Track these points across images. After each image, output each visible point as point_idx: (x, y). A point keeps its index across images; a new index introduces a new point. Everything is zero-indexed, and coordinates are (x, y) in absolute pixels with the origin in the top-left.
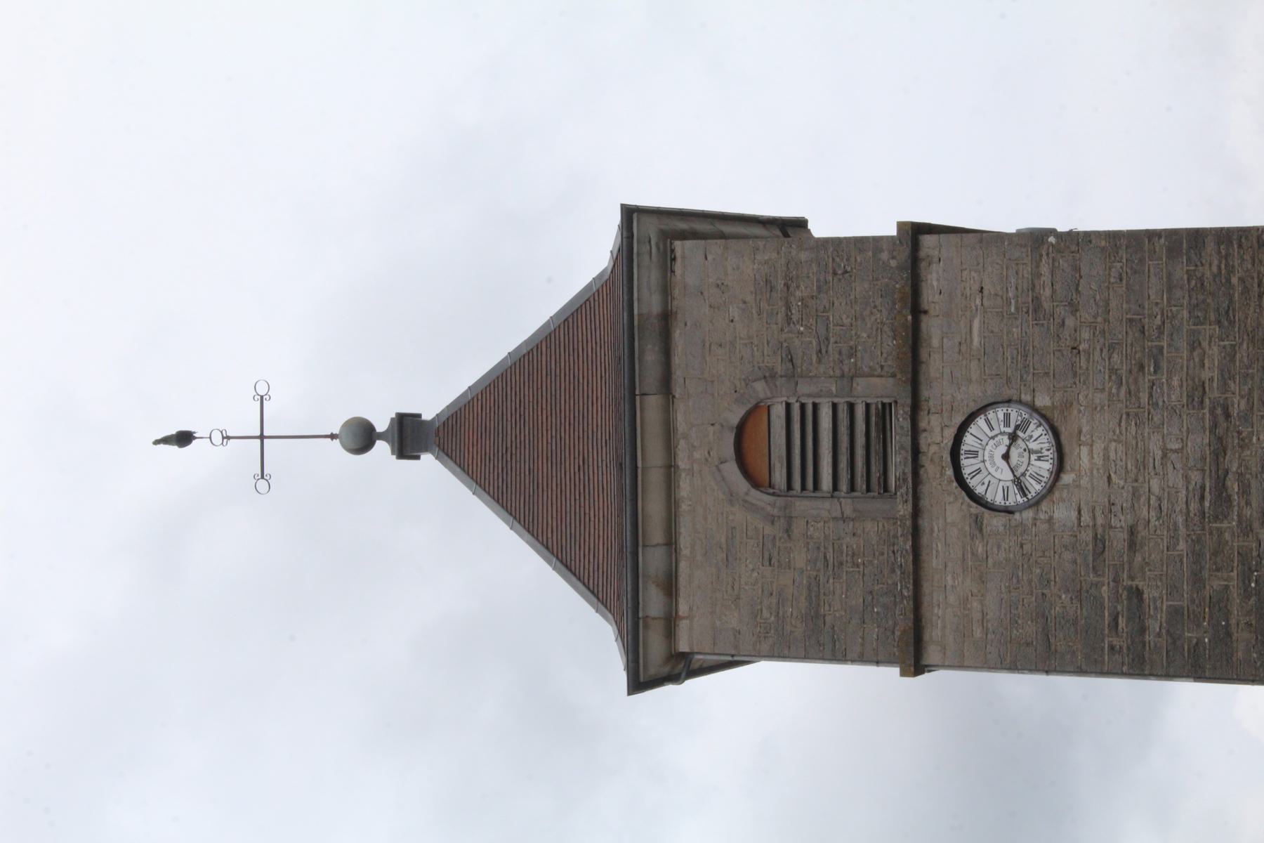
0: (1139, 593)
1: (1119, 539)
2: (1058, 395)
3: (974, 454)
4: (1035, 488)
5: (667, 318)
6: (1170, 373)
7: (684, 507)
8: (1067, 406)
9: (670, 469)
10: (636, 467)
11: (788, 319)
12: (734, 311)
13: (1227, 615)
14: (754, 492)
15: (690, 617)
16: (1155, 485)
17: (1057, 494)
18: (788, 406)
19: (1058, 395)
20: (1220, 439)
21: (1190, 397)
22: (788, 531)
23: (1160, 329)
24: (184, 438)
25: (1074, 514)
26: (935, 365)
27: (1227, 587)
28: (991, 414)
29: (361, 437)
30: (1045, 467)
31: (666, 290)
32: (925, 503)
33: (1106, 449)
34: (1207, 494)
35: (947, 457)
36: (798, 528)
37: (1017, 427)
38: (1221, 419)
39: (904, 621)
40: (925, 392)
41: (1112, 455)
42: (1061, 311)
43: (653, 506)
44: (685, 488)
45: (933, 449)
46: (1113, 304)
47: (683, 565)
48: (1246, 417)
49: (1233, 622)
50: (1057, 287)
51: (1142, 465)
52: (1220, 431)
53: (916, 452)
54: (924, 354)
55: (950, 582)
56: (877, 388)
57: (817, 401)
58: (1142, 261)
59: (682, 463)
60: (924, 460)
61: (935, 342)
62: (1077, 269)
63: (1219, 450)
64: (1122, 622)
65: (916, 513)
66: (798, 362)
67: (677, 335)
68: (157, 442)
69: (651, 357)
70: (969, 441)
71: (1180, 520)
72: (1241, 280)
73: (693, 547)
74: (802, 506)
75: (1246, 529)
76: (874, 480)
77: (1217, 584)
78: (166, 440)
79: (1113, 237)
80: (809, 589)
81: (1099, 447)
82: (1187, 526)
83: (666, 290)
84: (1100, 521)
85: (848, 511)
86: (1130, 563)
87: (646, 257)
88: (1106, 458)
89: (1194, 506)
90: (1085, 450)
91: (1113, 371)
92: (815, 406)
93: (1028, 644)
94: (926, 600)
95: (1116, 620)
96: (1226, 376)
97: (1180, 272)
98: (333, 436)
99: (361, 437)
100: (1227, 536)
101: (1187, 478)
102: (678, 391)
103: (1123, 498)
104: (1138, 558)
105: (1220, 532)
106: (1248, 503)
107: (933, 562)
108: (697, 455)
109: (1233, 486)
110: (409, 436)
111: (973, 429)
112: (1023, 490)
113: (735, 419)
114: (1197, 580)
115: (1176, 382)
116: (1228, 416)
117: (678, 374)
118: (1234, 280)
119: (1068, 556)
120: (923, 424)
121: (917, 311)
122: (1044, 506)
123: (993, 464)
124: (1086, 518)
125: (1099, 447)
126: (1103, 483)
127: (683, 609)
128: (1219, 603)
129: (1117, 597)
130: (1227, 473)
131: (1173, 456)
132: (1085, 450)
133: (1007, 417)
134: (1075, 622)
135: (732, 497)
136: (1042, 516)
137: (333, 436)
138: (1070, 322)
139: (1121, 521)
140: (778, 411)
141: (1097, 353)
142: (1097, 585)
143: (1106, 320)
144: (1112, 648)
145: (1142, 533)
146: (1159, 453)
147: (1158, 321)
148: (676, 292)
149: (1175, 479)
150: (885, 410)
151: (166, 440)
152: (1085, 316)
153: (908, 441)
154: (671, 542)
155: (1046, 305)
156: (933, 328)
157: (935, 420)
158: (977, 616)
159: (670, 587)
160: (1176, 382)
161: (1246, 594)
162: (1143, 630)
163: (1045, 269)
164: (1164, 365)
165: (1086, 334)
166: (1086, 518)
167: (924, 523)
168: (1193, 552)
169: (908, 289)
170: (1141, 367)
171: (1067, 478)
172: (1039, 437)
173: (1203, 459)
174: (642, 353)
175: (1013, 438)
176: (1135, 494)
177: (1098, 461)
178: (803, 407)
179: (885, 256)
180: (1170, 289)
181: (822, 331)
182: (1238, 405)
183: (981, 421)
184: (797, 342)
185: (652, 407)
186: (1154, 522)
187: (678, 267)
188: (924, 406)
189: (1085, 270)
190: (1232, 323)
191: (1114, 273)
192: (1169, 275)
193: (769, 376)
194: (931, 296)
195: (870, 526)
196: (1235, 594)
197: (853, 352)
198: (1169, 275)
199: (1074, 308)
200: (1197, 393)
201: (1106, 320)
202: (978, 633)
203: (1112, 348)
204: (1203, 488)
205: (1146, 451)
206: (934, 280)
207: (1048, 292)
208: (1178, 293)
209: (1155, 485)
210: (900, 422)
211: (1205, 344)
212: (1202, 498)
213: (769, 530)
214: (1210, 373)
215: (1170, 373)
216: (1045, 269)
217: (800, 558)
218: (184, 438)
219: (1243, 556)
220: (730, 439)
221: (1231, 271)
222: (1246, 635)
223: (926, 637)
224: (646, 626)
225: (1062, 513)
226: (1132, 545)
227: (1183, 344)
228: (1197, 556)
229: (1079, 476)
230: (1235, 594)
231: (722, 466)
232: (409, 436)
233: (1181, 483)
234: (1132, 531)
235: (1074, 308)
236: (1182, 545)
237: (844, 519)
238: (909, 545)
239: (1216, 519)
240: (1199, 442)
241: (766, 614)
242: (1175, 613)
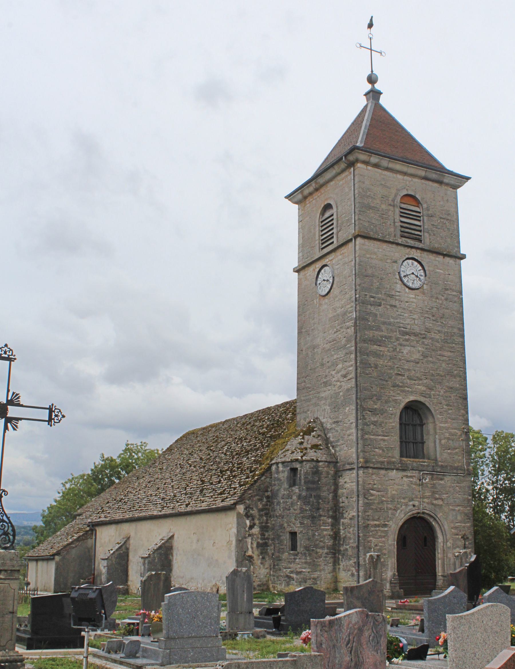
0: (380, 305)
1: (393, 302)
2: (426, 291)
3: (413, 264)
4: (405, 280)
5: (440, 183)
6: (433, 324)
7: (395, 175)
8: (424, 293)
9: (405, 174)
10: (409, 164)
11: (441, 218)
12: (441, 203)
13: (376, 330)
14: (400, 197)
15: (367, 169)
16: (406, 315)
17: (403, 286)
18: (420, 213)
19: (426, 291)
20: (418, 335)
21: (427, 328)
22: (390, 205)
23: (442, 323)
24: (370, 26)
25: (398, 290)
26: (432, 257)
27: (383, 331)
28: (422, 271)
29: (372, 80)
30: (410, 285)
31: (447, 184)
32: (400, 247)
33: (414, 303)
34: (405, 329)
35: (410, 256)
36: (391, 208)
37: (420, 278)
38: (422, 336)
39: (372, 234)
40: (425, 253)
41: (413, 304)
42: (445, 296)
43: (398, 166)
44: (400, 177)
45: (412, 253)
46: (447, 311)
47: (380, 171)
48: (423, 343)
49: (374, 332)
50: (451, 296)
51: (411, 312)
52: (420, 335)
53: (412, 247)
54: (434, 255)
55: (380, 250)
56: (427, 241)
57: (422, 222)
58: (457, 320)
59: (406, 178)
60: (410, 249)
61: (437, 259)
62: (455, 302)
63: (415, 335)
64: (372, 299)
65: (398, 244)
66: (431, 218)
67: (436, 185)
68: (372, 17)
69: (433, 175)
70: (416, 263)
71: (398, 321)
72: (454, 347)
73: (385, 175)
74: (397, 210)
75: (397, 339)
76: (405, 234)
77: (384, 328)
78: (371, 20)
79: (462, 313)
80: (376, 207)
81: (415, 300)
82: (397, 322)
83: (447, 184)
84: (397, 297)
85: (396, 224)
86: (387, 304)
87: (457, 181)
88: (412, 302)
89: (402, 325)
90: (414, 296)
91: (432, 308)
92: (420, 221)
93: (366, 270)
94: (375, 242)
95: (373, 297)
96: (432, 339)
97: (455, 330)
98: (372, 71)
99: (372, 80)
100: (395, 333)
101: (408, 324)
102: (423, 181)
103: (403, 305)
104: (388, 307)
105: (396, 332)
106: (403, 341)
107: (385, 246)
108: (408, 182)
109: (407, 337)
110: (374, 95)
111: (419, 265)
112: (405, 276)
113: (417, 196)
114: (384, 323)
115: (431, 325)
116: (424, 338)
117: (427, 182)
118: (454, 345)
119: (388, 286)
120: (418, 251)
121: (444, 255)
122: (400, 282)
123: (411, 269)
124: (398, 294)
125: (415, 300)
126: (406, 300)
127: (369, 168)
128: (379, 329)
129: (379, 299)
130: (410, 336)
131: (413, 321)
132: (414, 296)
133: (422, 276)
134: (372, 285)
135: (398, 190)
136: (398, 281)
137: (372, 71)
138: (443, 298)
139: (397, 303)
140: (418, 209)
141: (435, 304)
142: (381, 293)
143: (444, 308)
144: (366, 295)
145: (395, 309)
146: (414, 317)
147: (444, 323)
148: (446, 187)
149: (408, 321)
150: (420, 241)
151: (371, 20)
152: (445, 302)
153: (416, 246)
154: (387, 169)
155: (446, 292)
156: (440, 258)
157: (419, 255)
158: (372, 256)
159: (376, 166)
160: (431, 325)
161: (382, 337)
162: (371, 305)
163: (454, 293)
164: (434, 322)
165: (440, 302)
166: (398, 294)
167: (394, 246)
168: (391, 323)
169: (451, 254)
170: (433, 316)
171: (407, 290)
172: (417, 284)
173: (413, 330)
174: (436, 174)
175: (417, 276)
176: (404, 309)
177: (411, 300)
178: (420, 217)
179: (456, 249)
180: (452, 327)
181: (439, 227)
182: (426, 341)
183: (420, 268)
184: (436, 219)
185: (422, 173)
186: (398, 313)
187: (451, 189)
188: (422, 252)
189: (455, 304)
190: (444, 343)
191: (454, 312)
192: (454, 327)
193: (428, 209)
194: (447, 259)
195: (392, 230)
196: (381, 333)
197: (434, 235)
198: (454, 327)
199: (446, 299)
200: (428, 330)
201: (444, 308)
202: (368, 256)
203: (438, 309)
204: (406, 328)
205: (414, 314)
206: (451, 261)
207: (450, 293)
208: (451, 329)
209: (406, 315)
210: (417, 244)
211: (439, 335)
212: (404, 328)
213: (390, 199)
214: (433, 335)
215: (433, 324)
216: (454, 293)
217: (384, 207)
218: (370, 26)
219: (390, 337)
220: (413, 193)
221: (456, 344)
222: (371, 335)
223: (366, 240)
224: (369, 155)
225: (399, 286)
226: (391, 306)
227: (439, 328)
228: (390, 324)
229: (408, 294)
230: (381, 333)
231: (406, 190)
232: (374, 95)
233: (406, 322)
234: (395, 306)
235: (446, 299)
236: (392, 320)
237: (394, 222)
238: (391, 240)
239: (399, 331)
240: (417, 330)
241: (369, 193)
242: (376, 315)
